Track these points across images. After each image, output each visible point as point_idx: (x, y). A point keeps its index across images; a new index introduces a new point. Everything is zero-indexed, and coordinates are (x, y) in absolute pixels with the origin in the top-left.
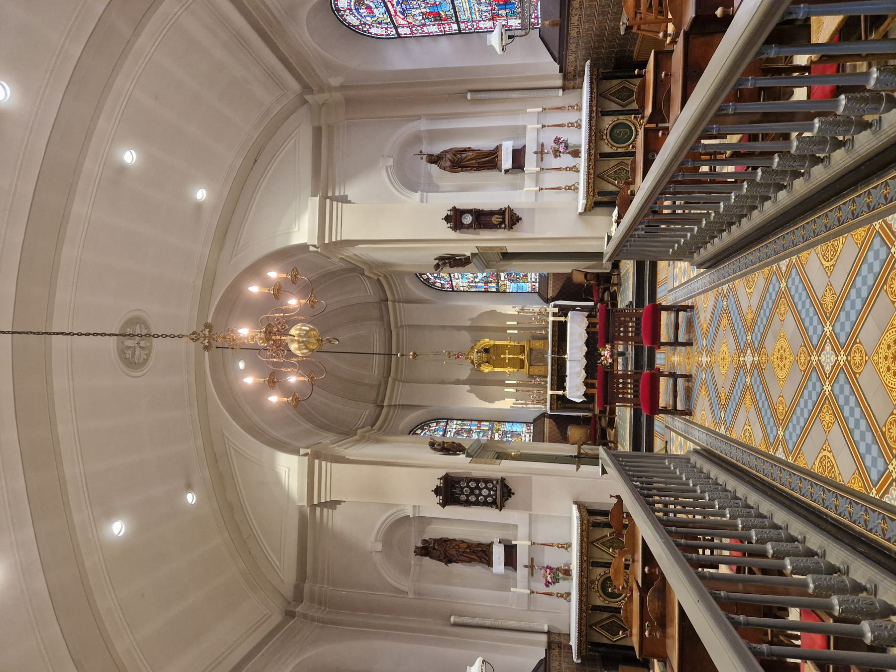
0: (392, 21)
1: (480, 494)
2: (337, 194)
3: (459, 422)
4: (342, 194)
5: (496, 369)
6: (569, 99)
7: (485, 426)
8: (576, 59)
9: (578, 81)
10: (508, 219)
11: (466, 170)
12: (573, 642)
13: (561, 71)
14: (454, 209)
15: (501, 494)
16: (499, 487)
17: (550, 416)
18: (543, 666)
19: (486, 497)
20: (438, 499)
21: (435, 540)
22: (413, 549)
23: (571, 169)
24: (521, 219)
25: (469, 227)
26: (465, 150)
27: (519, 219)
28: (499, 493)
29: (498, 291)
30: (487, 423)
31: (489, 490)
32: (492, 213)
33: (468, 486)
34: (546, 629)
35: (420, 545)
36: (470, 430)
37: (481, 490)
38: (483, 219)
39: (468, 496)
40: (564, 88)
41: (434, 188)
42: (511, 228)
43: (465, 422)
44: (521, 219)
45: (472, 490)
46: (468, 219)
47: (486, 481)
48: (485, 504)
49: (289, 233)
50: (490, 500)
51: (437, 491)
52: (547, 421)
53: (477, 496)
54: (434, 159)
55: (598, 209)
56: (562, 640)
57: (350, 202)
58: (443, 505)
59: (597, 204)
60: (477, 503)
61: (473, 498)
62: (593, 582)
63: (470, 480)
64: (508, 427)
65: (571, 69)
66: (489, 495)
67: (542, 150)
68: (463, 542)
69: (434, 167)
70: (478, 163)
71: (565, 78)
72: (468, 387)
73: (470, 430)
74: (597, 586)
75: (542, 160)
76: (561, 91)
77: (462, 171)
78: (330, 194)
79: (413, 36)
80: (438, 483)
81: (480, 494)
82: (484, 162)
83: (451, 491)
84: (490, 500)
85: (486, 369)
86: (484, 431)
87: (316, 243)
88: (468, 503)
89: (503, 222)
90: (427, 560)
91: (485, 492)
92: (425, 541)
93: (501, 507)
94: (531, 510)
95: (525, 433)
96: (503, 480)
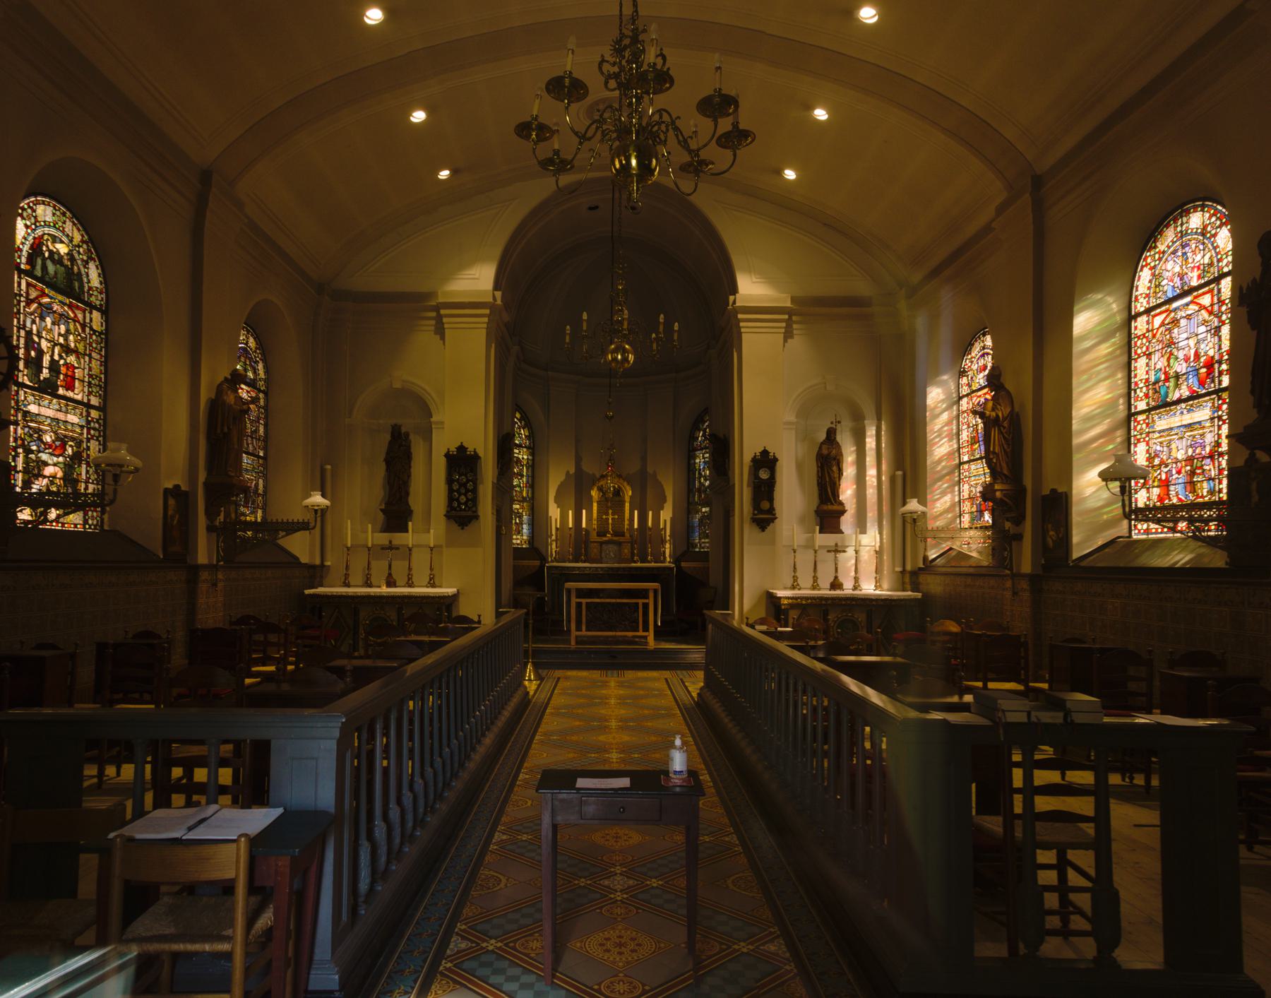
0: (973, 392)
2: (795, 326)
5: (595, 505)
9: (908, 587)
10: (764, 517)
13: (920, 569)
14: (775, 460)
15: (461, 514)
16: (470, 513)
17: (542, 567)
19: (458, 500)
20: (453, 449)
21: (409, 447)
25: (756, 476)
27: (763, 529)
28: (464, 513)
31: (465, 504)
33: (468, 481)
35: (403, 430)
36: (522, 476)
38: (764, 491)
40: (903, 572)
44: (763, 529)
45: (465, 485)
46: (764, 475)
49: (749, 270)
51: (462, 448)
52: (537, 563)
54: (831, 433)
57: (785, 341)
58: (447, 455)
60: (450, 491)
61: (455, 486)
66: (460, 504)
68: (409, 476)
71: (915, 573)
72: (572, 471)
73: (522, 476)
78: (794, 318)
80: (471, 449)
81: (460, 494)
83: (462, 463)
84: (456, 504)
86: (521, 492)
87: (738, 304)
88: (450, 481)
89: (762, 512)
90: (388, 437)
93: (448, 516)
94: (447, 546)
95: (520, 539)
96: (477, 517)
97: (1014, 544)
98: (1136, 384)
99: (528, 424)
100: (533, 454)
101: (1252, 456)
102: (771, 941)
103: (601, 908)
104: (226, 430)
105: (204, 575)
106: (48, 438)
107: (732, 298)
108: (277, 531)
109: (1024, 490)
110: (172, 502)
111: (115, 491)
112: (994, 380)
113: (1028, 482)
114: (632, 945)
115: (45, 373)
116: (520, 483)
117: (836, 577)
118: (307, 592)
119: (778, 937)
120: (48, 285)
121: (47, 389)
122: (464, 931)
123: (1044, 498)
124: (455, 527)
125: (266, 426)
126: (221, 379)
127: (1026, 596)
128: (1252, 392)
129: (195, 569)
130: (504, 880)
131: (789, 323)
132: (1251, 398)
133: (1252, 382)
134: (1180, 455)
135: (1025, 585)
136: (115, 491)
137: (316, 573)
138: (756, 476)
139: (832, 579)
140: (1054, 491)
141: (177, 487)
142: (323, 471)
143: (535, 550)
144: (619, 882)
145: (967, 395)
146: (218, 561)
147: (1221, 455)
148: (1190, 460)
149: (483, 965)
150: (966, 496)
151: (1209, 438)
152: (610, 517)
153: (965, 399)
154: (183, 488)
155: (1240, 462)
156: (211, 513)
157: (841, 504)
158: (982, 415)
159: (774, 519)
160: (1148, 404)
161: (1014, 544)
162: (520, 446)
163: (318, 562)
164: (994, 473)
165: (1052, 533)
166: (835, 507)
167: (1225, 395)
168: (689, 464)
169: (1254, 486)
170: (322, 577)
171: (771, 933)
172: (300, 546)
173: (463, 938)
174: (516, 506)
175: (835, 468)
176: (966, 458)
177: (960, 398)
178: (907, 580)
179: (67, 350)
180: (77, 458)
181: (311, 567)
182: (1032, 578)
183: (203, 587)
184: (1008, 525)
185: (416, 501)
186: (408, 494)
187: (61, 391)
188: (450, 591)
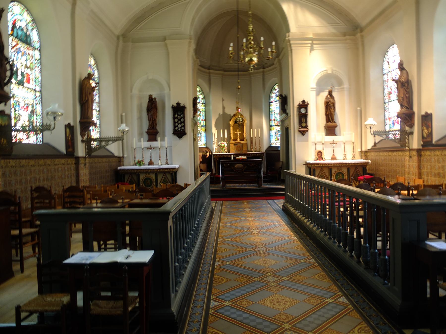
1: (179, 124)
3: (204, 110)
4: (315, 48)
6: (358, 155)
7: (203, 123)
8: (372, 156)
9: (364, 157)
10: (303, 129)
12: (122, 168)
13: (368, 150)
14: (308, 104)
18: (111, 154)
19: (177, 126)
20: (175, 105)
22: (151, 93)
25: (300, 112)
26: (334, 108)
27: (303, 135)
29: (271, 126)
30: (204, 124)
31: (181, 128)
32: (306, 122)
34: (125, 156)
35: (153, 97)
37: (180, 124)
38: (303, 118)
39: (177, 118)
40: (361, 152)
41: (318, 94)
43: (204, 113)
44: (303, 135)
46: (303, 111)
47: (184, 126)
48: (175, 126)
50: (176, 128)
51: (178, 104)
53: (177, 122)
54: (330, 93)
55: (308, 170)
56: (122, 163)
57: (310, 52)
58: (173, 107)
59: (310, 169)
60: (175, 123)
61: (176, 120)
62: (149, 174)
63: (184, 118)
64: (203, 134)
65: (369, 154)
71: (366, 152)
74: (148, 176)
75: (331, 144)
76: (360, 150)
78: (314, 42)
82: (329, 117)
83: (179, 110)
85: (231, 123)
86: (201, 123)
88: (174, 118)
89: (302, 127)
90: (148, 101)
91: (180, 126)
92: (155, 98)
95: (202, 143)
99: (203, 93)
100: (205, 106)
102: (340, 297)
103: (267, 289)
104: (87, 99)
105: (81, 161)
106: (22, 104)
107: (287, 34)
108: (109, 141)
109: (413, 113)
110: (68, 130)
111: (55, 124)
112: (401, 67)
113: (415, 109)
114: (274, 302)
115: (20, 77)
116: (201, 119)
117: (334, 155)
118: (119, 168)
119: (342, 296)
120: (20, 40)
121: (20, 83)
122: (214, 298)
124: (176, 138)
125: (99, 97)
126: (83, 78)
127: (415, 158)
129: (77, 158)
130: (225, 280)
131: (312, 44)
135: (415, 153)
136: (55, 124)
137: (120, 160)
139: (331, 156)
140: (426, 113)
141: (69, 124)
142: (122, 116)
143: (207, 148)
144: (271, 279)
146: (86, 155)
149: (226, 311)
152: (238, 133)
154: (72, 124)
156: (82, 135)
157: (335, 122)
158: (396, 81)
159: (307, 131)
161: (410, 136)
162: (199, 103)
163: (121, 155)
164: (402, 106)
165: (426, 131)
166: (333, 124)
168: (270, 109)
170: (123, 162)
171: (339, 295)
172: (114, 148)
173: (215, 301)
174: (199, 129)
175: (332, 108)
178: (363, 155)
179: (26, 67)
180: (33, 112)
181: (119, 158)
183: (81, 166)
184: (407, 128)
185: (159, 128)
186: (156, 124)
187: (26, 84)
188: (177, 166)
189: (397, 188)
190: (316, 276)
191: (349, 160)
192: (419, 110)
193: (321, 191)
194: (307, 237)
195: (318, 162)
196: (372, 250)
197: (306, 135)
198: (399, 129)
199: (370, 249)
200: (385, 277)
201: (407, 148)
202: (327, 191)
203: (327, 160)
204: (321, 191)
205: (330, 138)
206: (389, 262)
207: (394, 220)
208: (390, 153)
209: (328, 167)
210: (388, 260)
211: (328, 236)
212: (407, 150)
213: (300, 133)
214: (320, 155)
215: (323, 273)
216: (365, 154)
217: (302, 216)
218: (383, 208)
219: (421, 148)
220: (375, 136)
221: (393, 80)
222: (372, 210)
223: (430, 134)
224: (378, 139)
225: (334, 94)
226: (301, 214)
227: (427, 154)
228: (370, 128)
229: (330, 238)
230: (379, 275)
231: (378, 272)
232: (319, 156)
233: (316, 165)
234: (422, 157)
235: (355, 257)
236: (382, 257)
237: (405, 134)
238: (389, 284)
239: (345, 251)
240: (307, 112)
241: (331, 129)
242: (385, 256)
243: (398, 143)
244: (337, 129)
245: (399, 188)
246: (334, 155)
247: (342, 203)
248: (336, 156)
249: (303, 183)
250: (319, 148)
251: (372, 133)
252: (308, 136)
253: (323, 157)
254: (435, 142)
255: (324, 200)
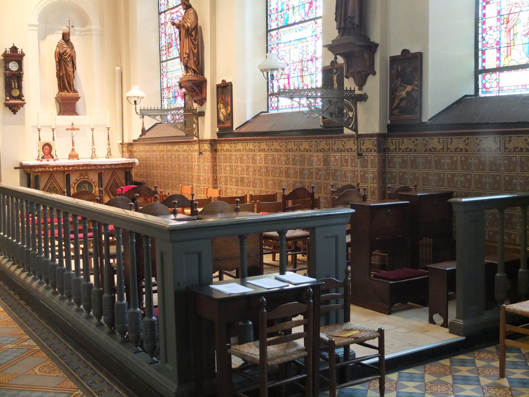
8: (140, 151)
9: (127, 155)
11: (57, 66)
13: (134, 141)
23: (109, 152)
24: (15, 113)
25: (7, 68)
26: (74, 65)
27: (14, 112)
32: (20, 88)
40: (122, 144)
41: (43, 36)
42: (7, 105)
44: (14, 112)
46: (13, 66)
65: (135, 148)
67: (75, 129)
69: (59, 37)
70: (63, 76)
71: (130, 144)
75: (67, 129)
76: (121, 142)
77: (57, 62)
79: (160, 24)
82: (63, 81)
97: (200, 119)
98: (271, 10)
101: (336, 58)
109: (205, 81)
113: (207, 74)
117: (73, 150)
123: (218, 86)
127: (208, 154)
128: (336, 20)
132: (335, 23)
133: (336, 14)
134: (296, 59)
138: (7, 68)
139: (69, 151)
145: (165, 12)
147: (317, 59)
148: (302, 61)
150: (165, 86)
151: (311, 49)
153: (163, 15)
155: (328, 64)
157: (75, 91)
158: (178, 27)
159: (22, 105)
160: (277, 25)
161: (200, 119)
164: (187, 68)
165: (223, 110)
166: (71, 94)
167: (320, 21)
169: (335, 78)
175: (70, 65)
176: (164, 58)
177: (160, 14)
178: (125, 149)
182: (213, 143)
184: (195, 105)
189: (174, 203)
190: (36, 370)
191: (101, 160)
192: (213, 77)
193: (45, 214)
194: (22, 302)
195: (44, 162)
196: (132, 310)
197: (19, 112)
198: (183, 106)
199: (129, 308)
200: (153, 352)
201: (195, 138)
202: (55, 213)
203: (61, 158)
204: (45, 214)
205: (67, 120)
206: (158, 325)
207: (162, 254)
208: (169, 147)
209: (64, 172)
210: (156, 323)
211: (60, 295)
212: (196, 141)
213: (8, 108)
214: (47, 149)
215: (49, 362)
216: (128, 147)
217: (11, 263)
218: (147, 237)
219: (216, 138)
220: (143, 117)
221: (173, 24)
222: (130, 240)
223: (230, 116)
224: (149, 122)
225: (73, 39)
226: (9, 261)
227: (225, 148)
228: (135, 102)
229: (62, 299)
230: (144, 351)
231: (141, 346)
232: (47, 151)
233: (40, 169)
234: (218, 153)
235: (106, 325)
236: (146, 319)
237: (192, 116)
238: (160, 362)
239: (89, 317)
240: (20, 68)
241: (68, 104)
242: (151, 316)
243: (181, 129)
244: (79, 104)
245: (175, 203)
246: (73, 150)
247: (81, 235)
248: (77, 151)
249: (12, 202)
250: (47, 138)
251: (138, 111)
252: (24, 114)
253: (53, 153)
254: (236, 129)
255: (49, 231)
